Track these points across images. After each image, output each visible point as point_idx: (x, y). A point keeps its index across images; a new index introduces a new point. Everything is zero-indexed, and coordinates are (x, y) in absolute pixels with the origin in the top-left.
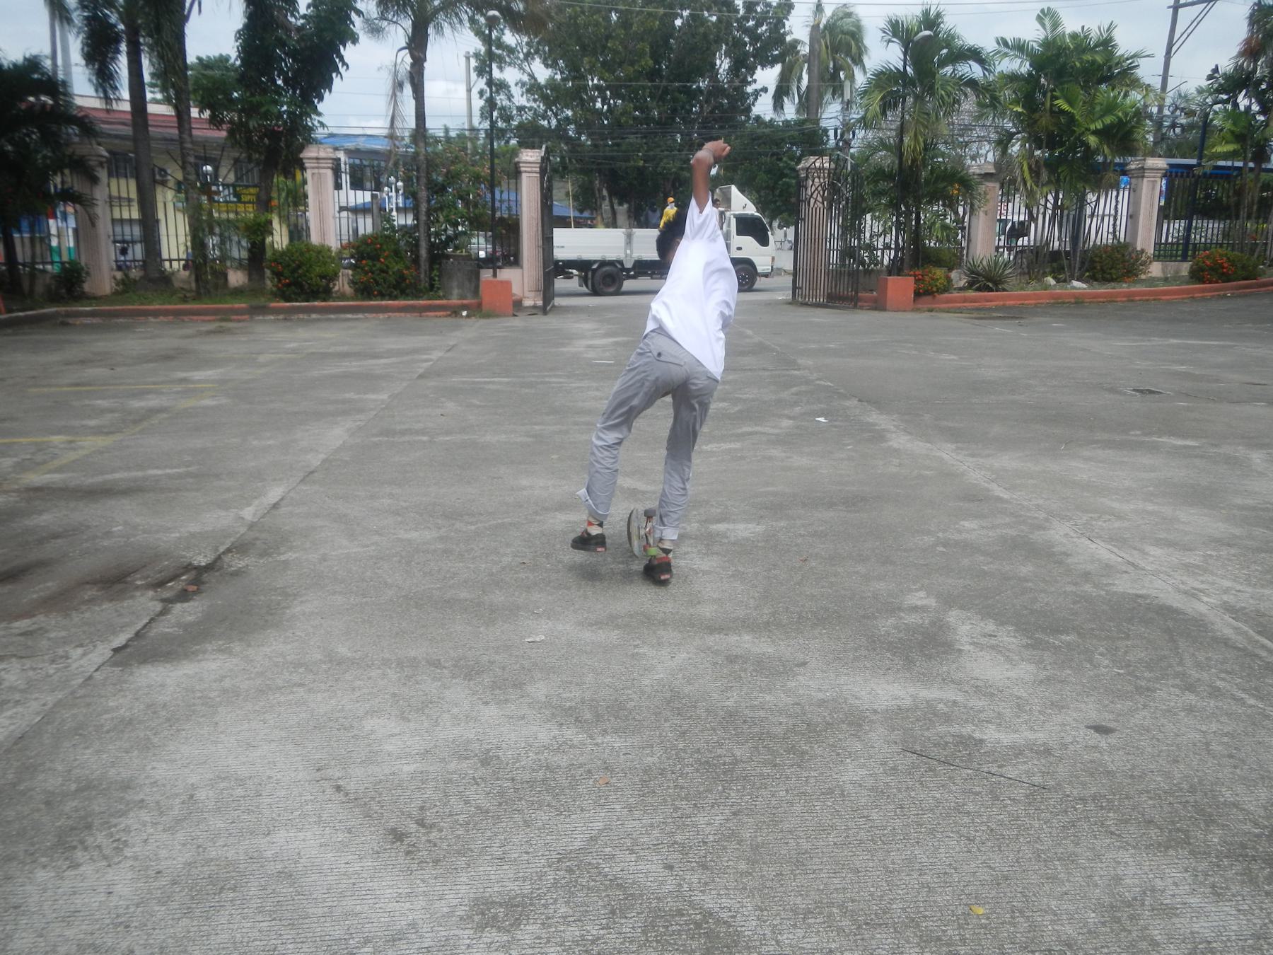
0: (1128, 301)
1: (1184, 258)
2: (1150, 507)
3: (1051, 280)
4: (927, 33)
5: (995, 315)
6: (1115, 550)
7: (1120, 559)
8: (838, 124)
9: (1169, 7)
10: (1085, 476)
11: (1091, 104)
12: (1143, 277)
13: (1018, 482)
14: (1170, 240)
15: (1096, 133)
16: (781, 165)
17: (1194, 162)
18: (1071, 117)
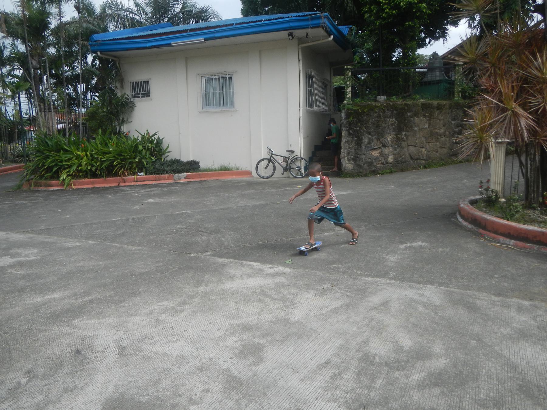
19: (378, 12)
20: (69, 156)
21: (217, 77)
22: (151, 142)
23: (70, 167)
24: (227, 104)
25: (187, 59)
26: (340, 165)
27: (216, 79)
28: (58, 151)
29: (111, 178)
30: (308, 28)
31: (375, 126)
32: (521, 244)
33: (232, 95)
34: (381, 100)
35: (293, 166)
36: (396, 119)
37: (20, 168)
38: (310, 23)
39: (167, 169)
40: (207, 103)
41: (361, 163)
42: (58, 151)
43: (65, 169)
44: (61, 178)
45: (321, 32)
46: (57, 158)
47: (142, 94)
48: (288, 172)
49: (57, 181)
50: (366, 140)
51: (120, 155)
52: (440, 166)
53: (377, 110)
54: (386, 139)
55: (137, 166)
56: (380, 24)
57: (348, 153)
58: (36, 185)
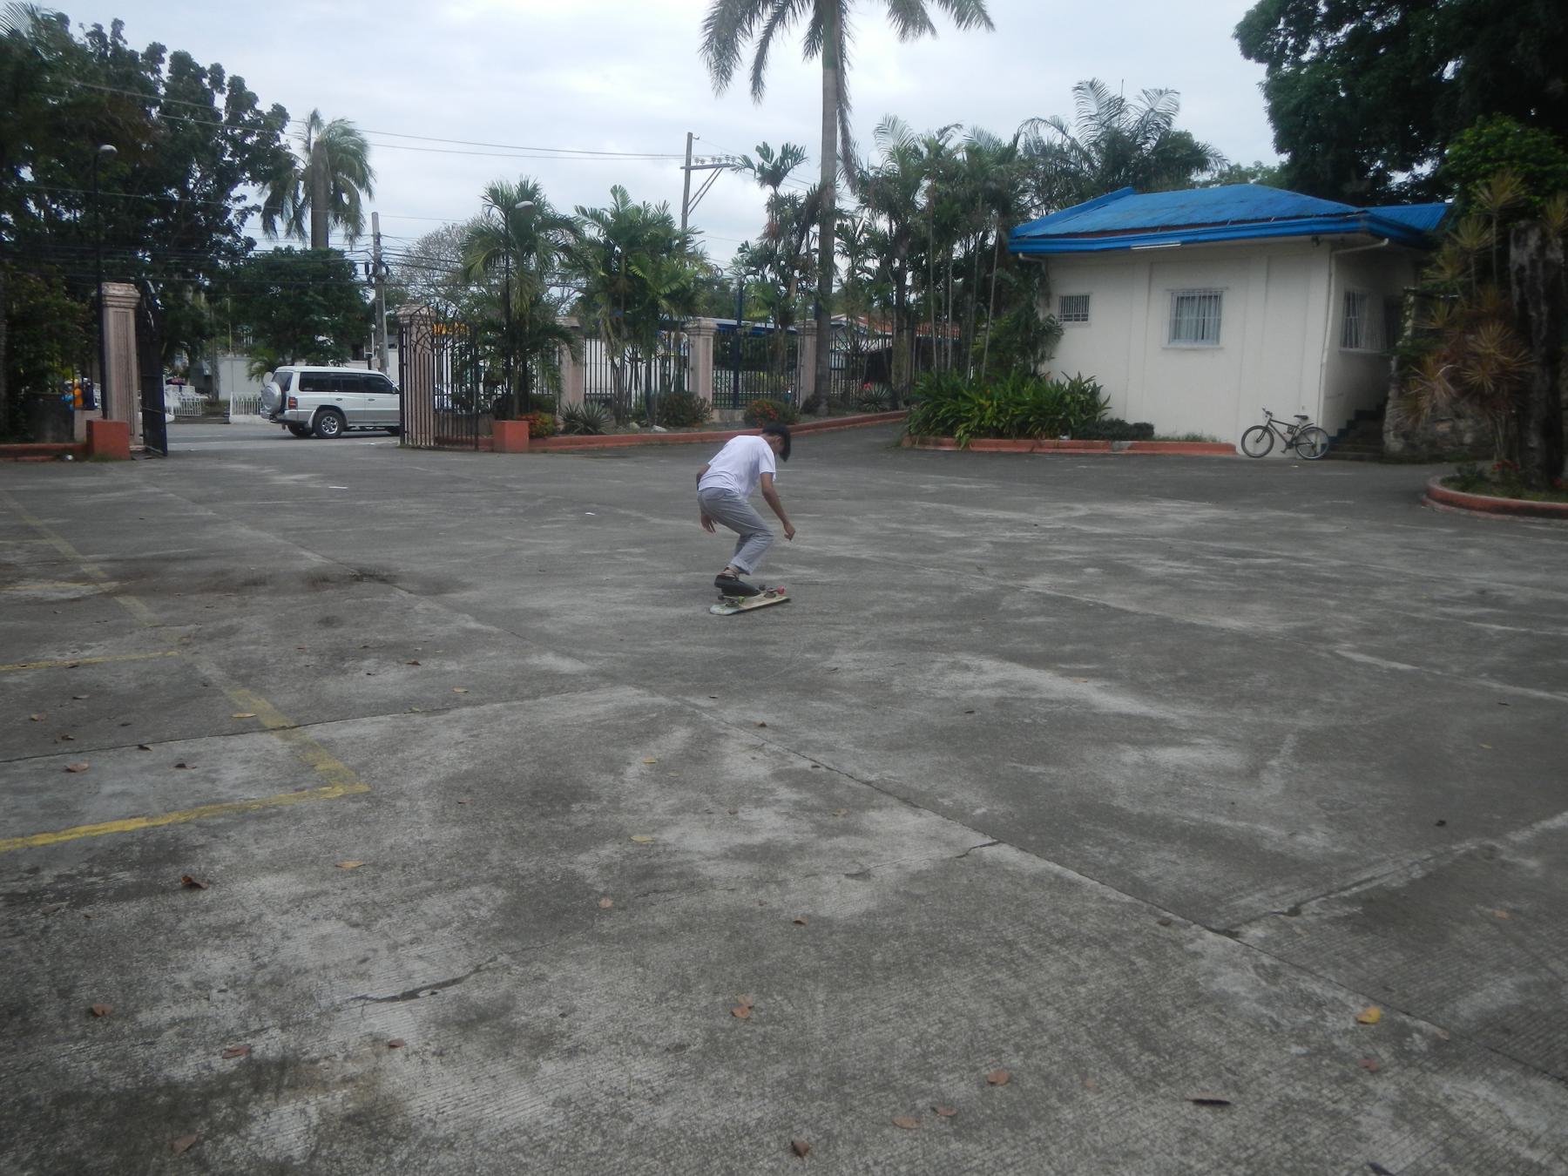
1: (735, 406)
3: (635, 425)
4: (529, 203)
8: (369, 258)
11: (658, 271)
12: (707, 422)
15: (666, 297)
16: (307, 299)
17: (734, 322)
20: (969, 406)
21: (1196, 294)
22: (1084, 392)
23: (969, 419)
26: (1383, 443)
27: (1194, 298)
28: (955, 397)
29: (1022, 441)
32: (1447, 507)
35: (1303, 440)
37: (871, 419)
38: (1342, 226)
40: (1176, 333)
42: (955, 397)
48: (1294, 450)
51: (1040, 408)
58: (923, 442)
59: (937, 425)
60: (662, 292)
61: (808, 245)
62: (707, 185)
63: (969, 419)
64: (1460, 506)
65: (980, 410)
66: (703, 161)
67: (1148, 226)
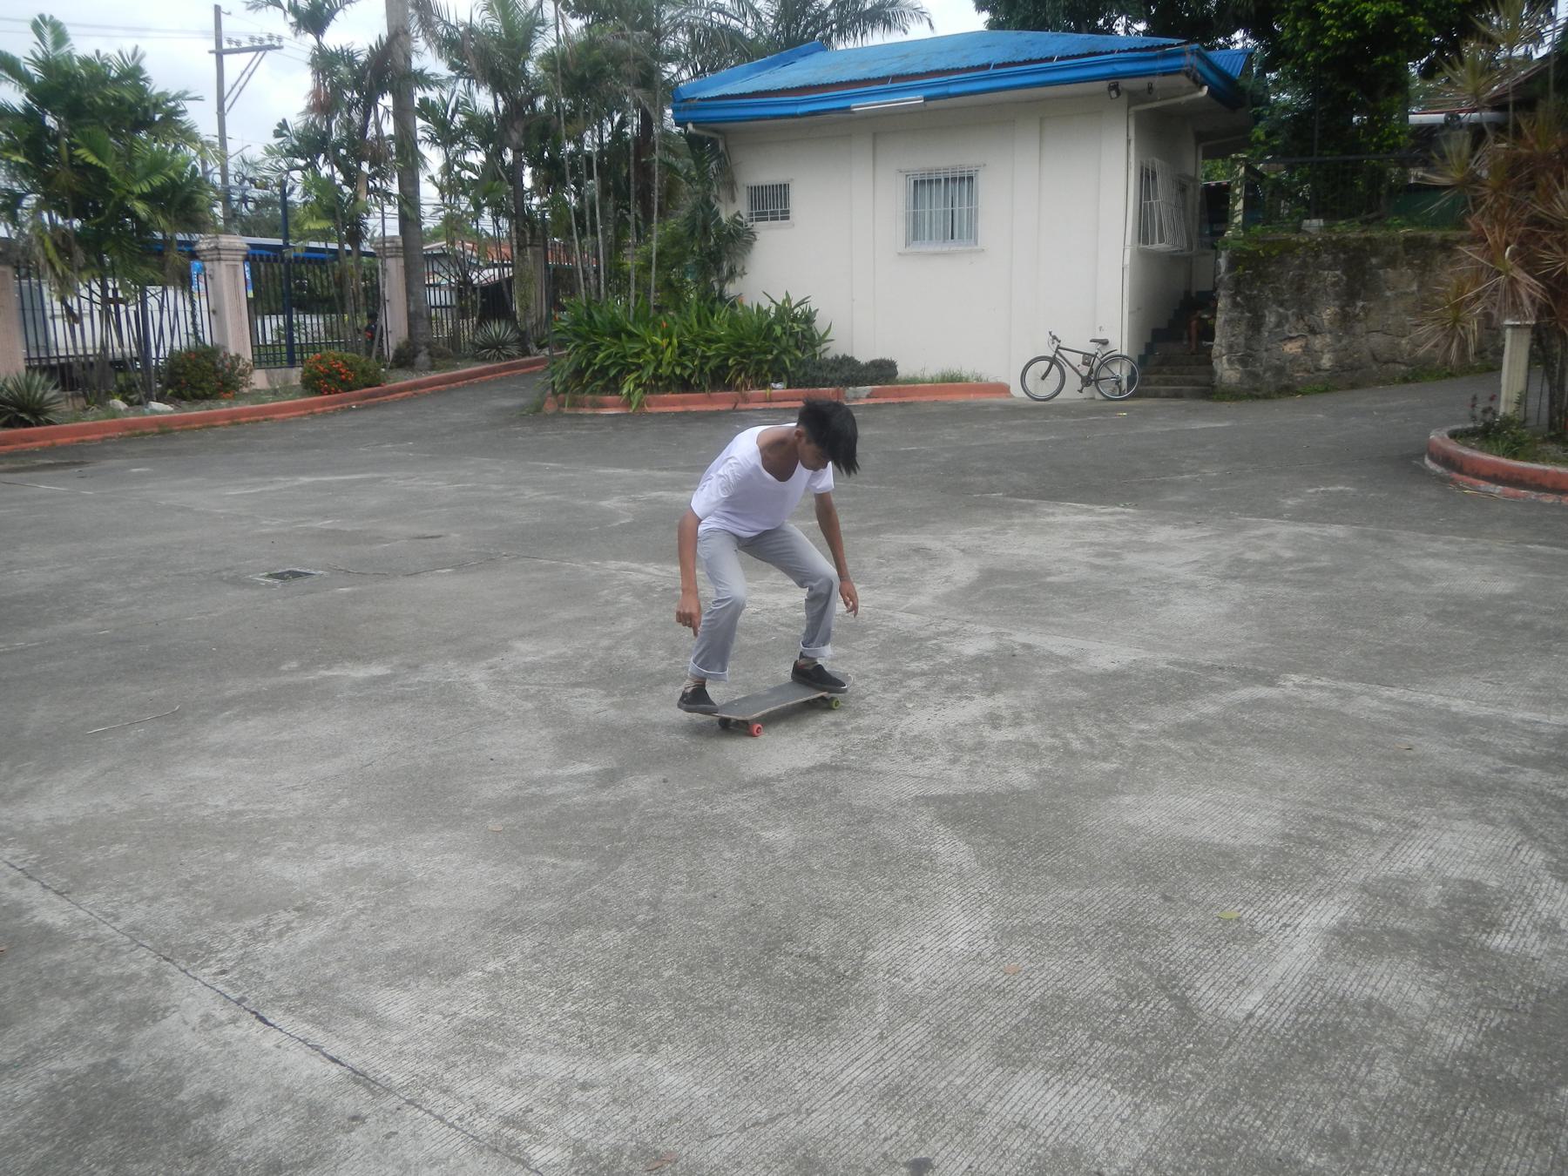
0: (233, 424)
1: (292, 363)
2: (358, 857)
3: (119, 404)
5: (40, 461)
6: (319, 1037)
7: (334, 1069)
9: (211, 52)
10: (222, 802)
11: (129, 155)
12: (245, 390)
13: (88, 858)
14: (268, 337)
15: (142, 197)
17: (279, 242)
18: (102, 175)
19: (1312, 34)
20: (638, 347)
22: (795, 319)
23: (639, 367)
24: (960, 237)
25: (875, 135)
26: (1212, 373)
27: (938, 181)
30: (1154, 75)
31: (1294, 287)
32: (1511, 491)
33: (972, 217)
34: (1311, 230)
35: (1104, 373)
36: (1344, 272)
37: (493, 371)
39: (831, 376)
40: (916, 231)
41: (1260, 370)
43: (630, 372)
44: (625, 391)
45: (1183, 80)
46: (614, 350)
47: (772, 213)
49: (617, 397)
50: (1271, 319)
51: (740, 345)
52: (1439, 378)
53: (1300, 251)
54: (1319, 315)
55: (769, 370)
56: (1316, 59)
57: (1230, 347)
58: (574, 404)
59: (594, 377)
60: (137, 189)
61: (378, 125)
62: (248, 73)
63: (639, 367)
64: (1540, 488)
65: (653, 352)
66: (238, 43)
67: (875, 75)
